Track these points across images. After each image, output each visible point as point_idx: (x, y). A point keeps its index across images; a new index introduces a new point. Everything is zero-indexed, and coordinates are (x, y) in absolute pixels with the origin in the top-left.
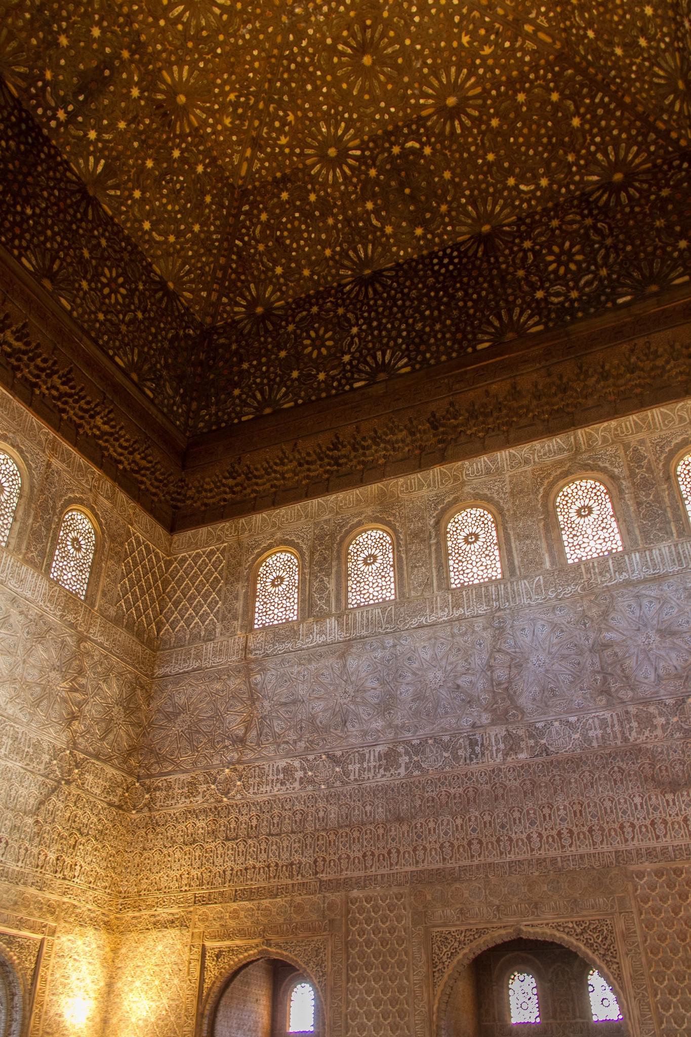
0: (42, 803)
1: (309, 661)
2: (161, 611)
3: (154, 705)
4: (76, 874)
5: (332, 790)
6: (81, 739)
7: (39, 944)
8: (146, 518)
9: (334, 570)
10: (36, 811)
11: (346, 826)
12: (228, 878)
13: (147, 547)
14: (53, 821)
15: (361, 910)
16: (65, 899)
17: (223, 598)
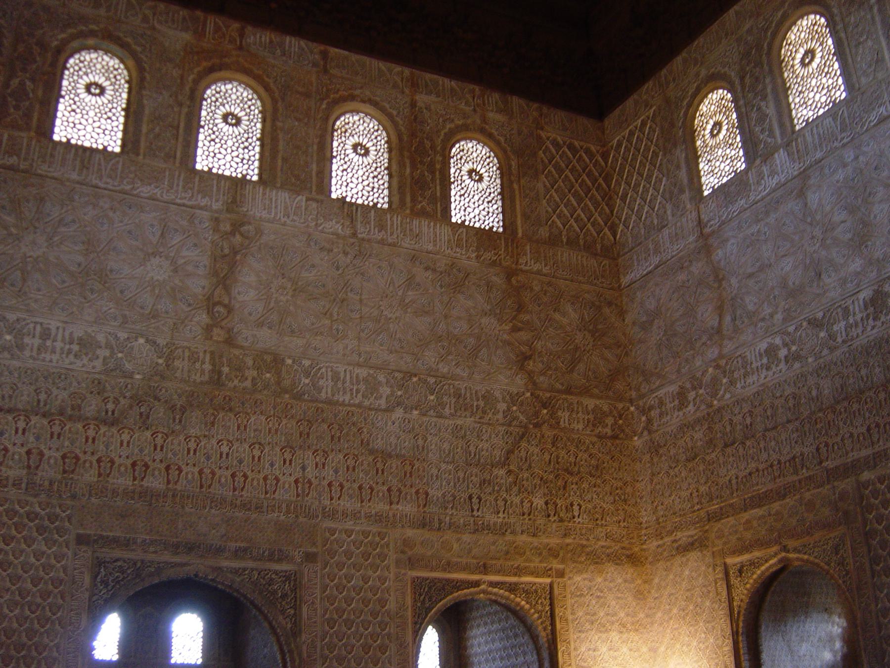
0: (510, 452)
1: (767, 213)
2: (612, 212)
3: (629, 319)
4: (576, 514)
5: (822, 360)
6: (542, 378)
7: (548, 588)
8: (559, 115)
9: (769, 90)
10: (505, 463)
11: (843, 400)
12: (735, 487)
13: (571, 147)
14: (530, 466)
15: (875, 493)
16: (568, 541)
17: (665, 172)
